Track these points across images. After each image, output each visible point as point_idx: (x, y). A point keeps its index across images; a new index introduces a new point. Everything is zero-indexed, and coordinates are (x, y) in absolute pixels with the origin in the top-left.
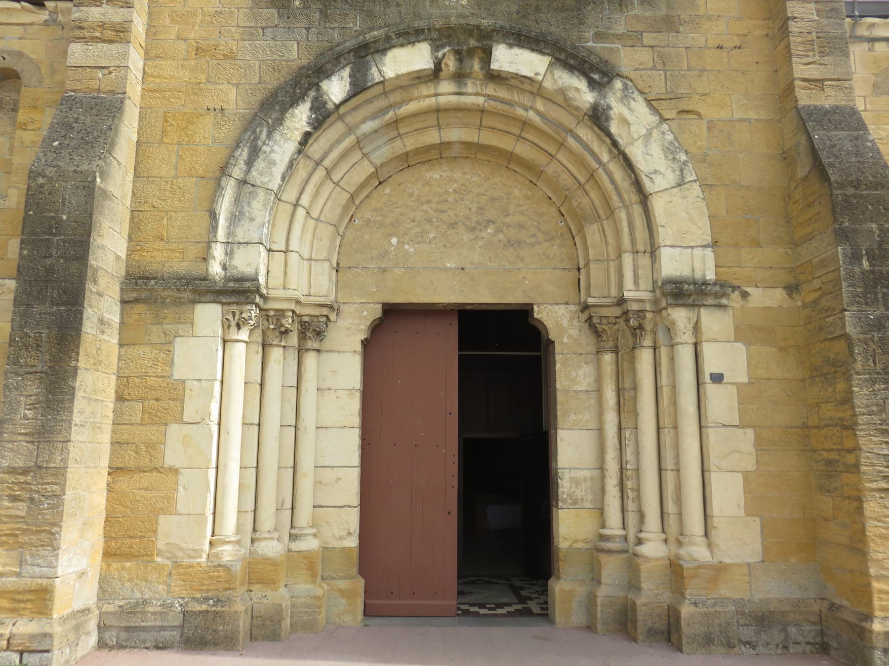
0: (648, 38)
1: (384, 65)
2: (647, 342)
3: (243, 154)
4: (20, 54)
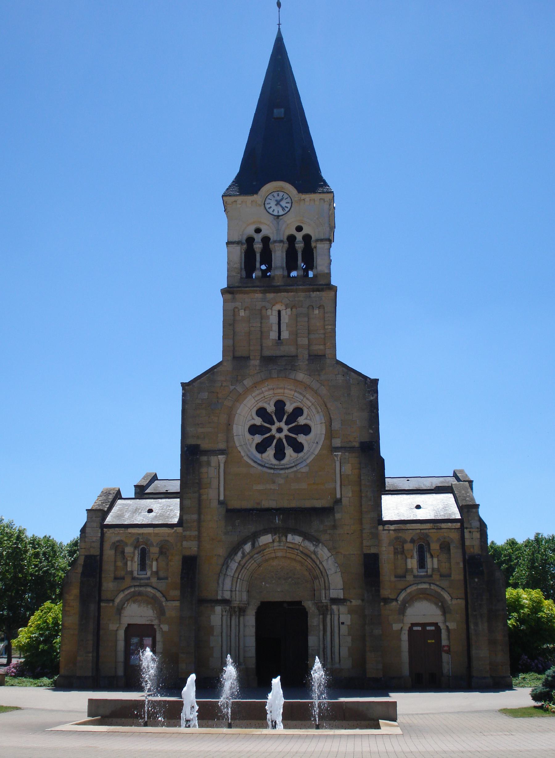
0: (329, 532)
2: (329, 613)
4: (168, 541)
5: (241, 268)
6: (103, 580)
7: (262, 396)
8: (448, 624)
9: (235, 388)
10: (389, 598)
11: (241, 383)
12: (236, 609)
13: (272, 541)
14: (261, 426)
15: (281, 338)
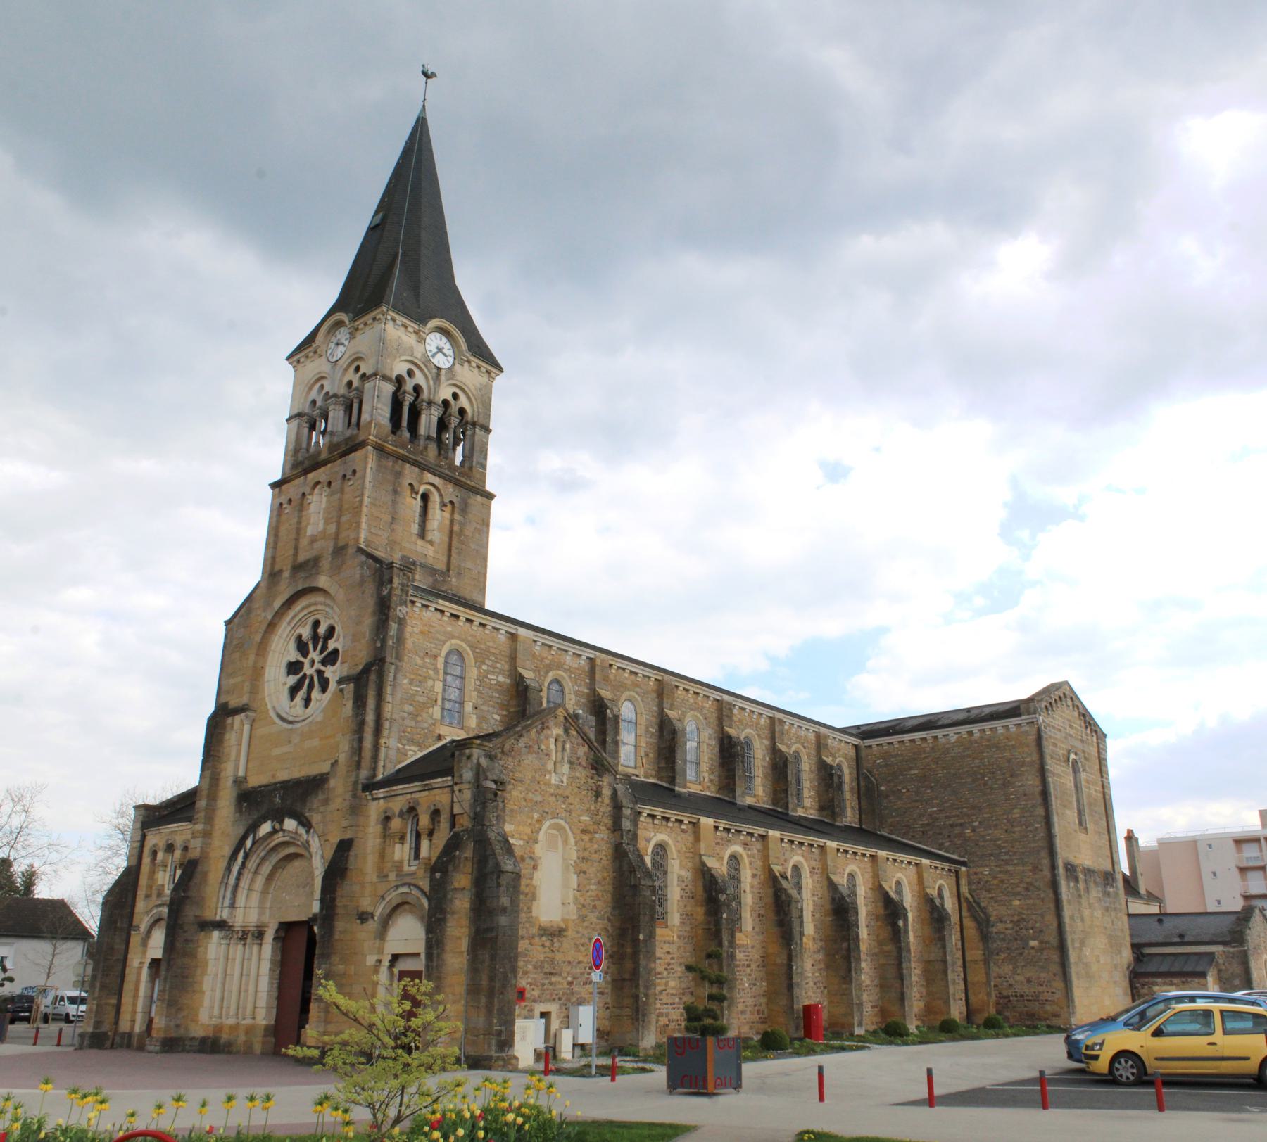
0: (322, 809)
7: (297, 619)
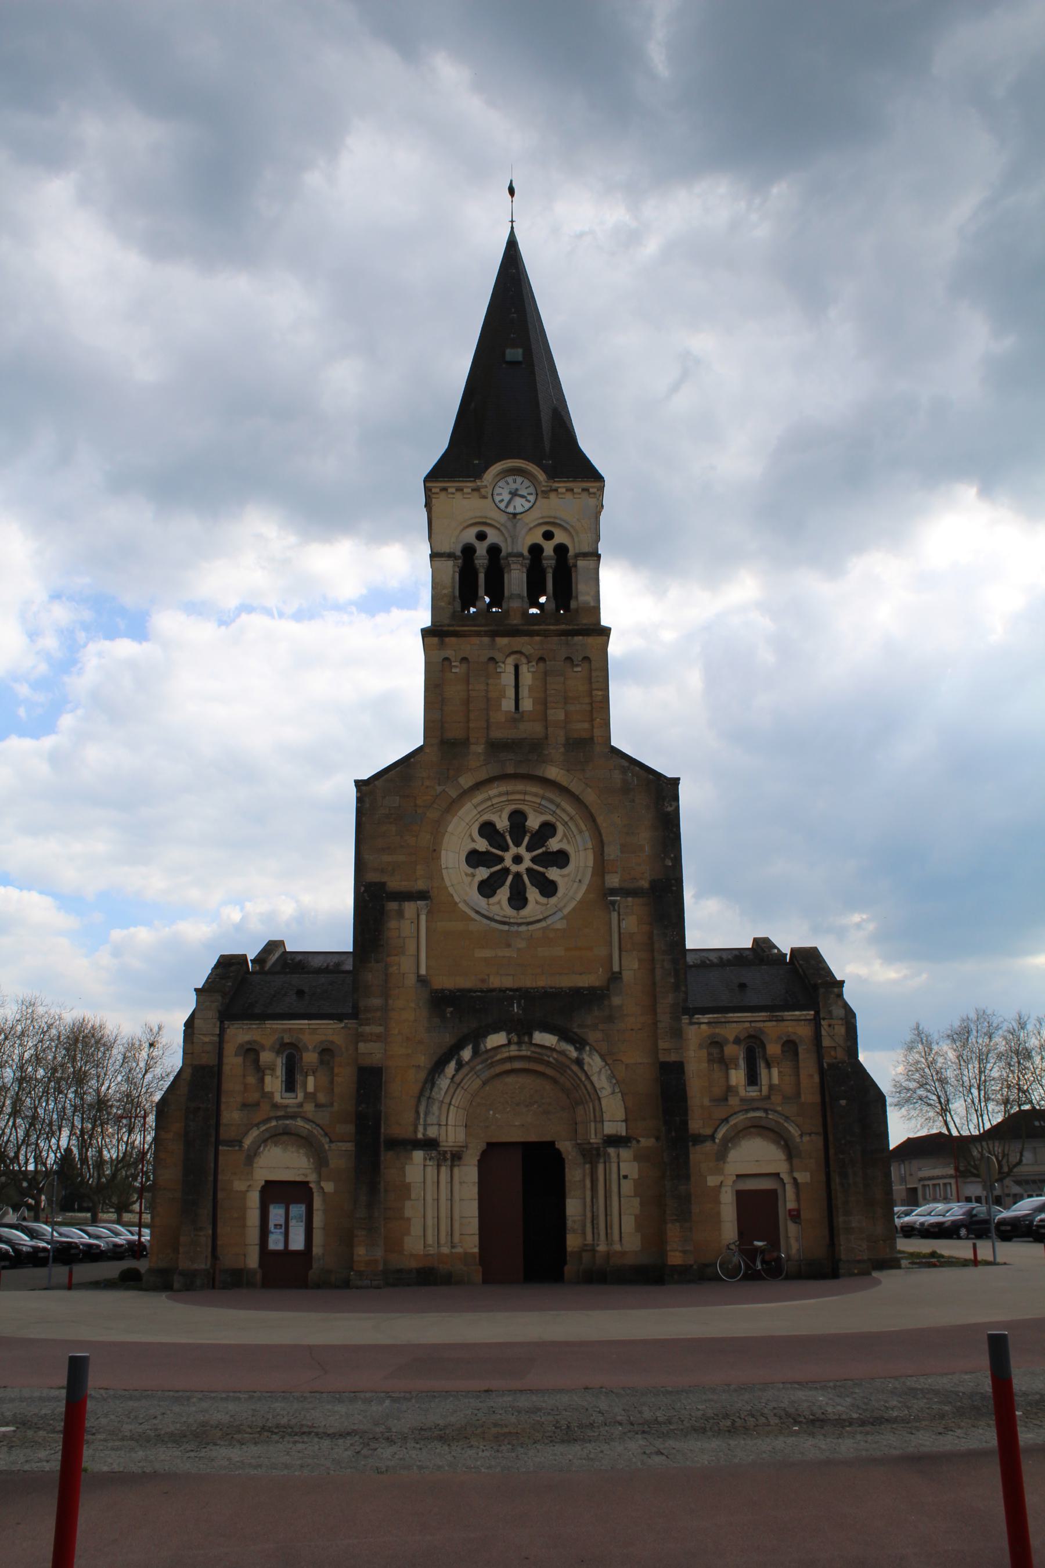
1: (486, 1043)
2: (602, 1160)
3: (428, 1086)
4: (332, 1042)
5: (454, 597)
6: (223, 1107)
7: (489, 803)
8: (796, 1175)
9: (444, 790)
10: (699, 1135)
11: (455, 782)
12: (449, 1156)
13: (507, 1042)
14: (487, 853)
15: (521, 709)
